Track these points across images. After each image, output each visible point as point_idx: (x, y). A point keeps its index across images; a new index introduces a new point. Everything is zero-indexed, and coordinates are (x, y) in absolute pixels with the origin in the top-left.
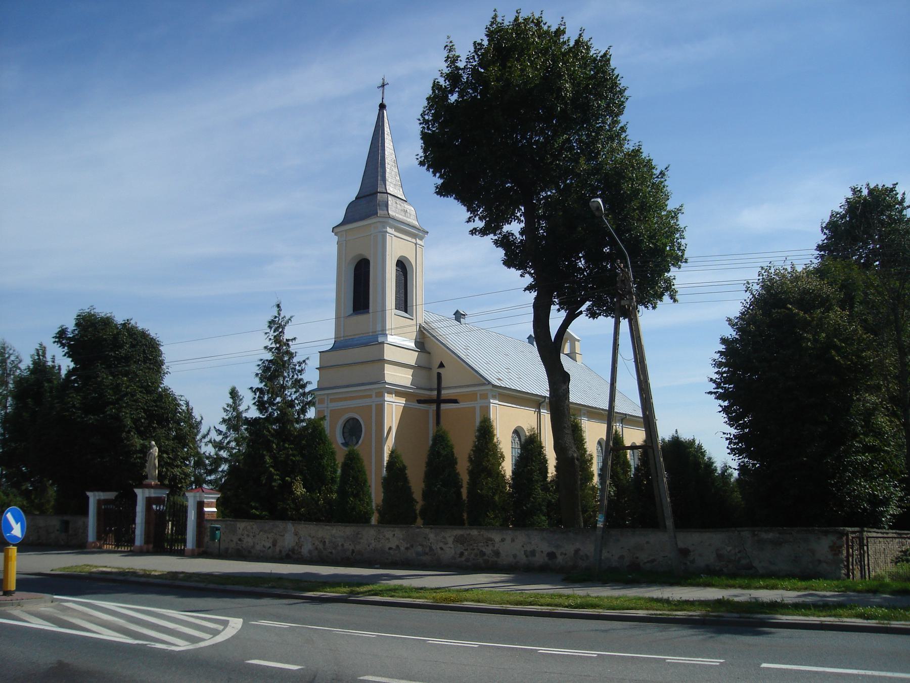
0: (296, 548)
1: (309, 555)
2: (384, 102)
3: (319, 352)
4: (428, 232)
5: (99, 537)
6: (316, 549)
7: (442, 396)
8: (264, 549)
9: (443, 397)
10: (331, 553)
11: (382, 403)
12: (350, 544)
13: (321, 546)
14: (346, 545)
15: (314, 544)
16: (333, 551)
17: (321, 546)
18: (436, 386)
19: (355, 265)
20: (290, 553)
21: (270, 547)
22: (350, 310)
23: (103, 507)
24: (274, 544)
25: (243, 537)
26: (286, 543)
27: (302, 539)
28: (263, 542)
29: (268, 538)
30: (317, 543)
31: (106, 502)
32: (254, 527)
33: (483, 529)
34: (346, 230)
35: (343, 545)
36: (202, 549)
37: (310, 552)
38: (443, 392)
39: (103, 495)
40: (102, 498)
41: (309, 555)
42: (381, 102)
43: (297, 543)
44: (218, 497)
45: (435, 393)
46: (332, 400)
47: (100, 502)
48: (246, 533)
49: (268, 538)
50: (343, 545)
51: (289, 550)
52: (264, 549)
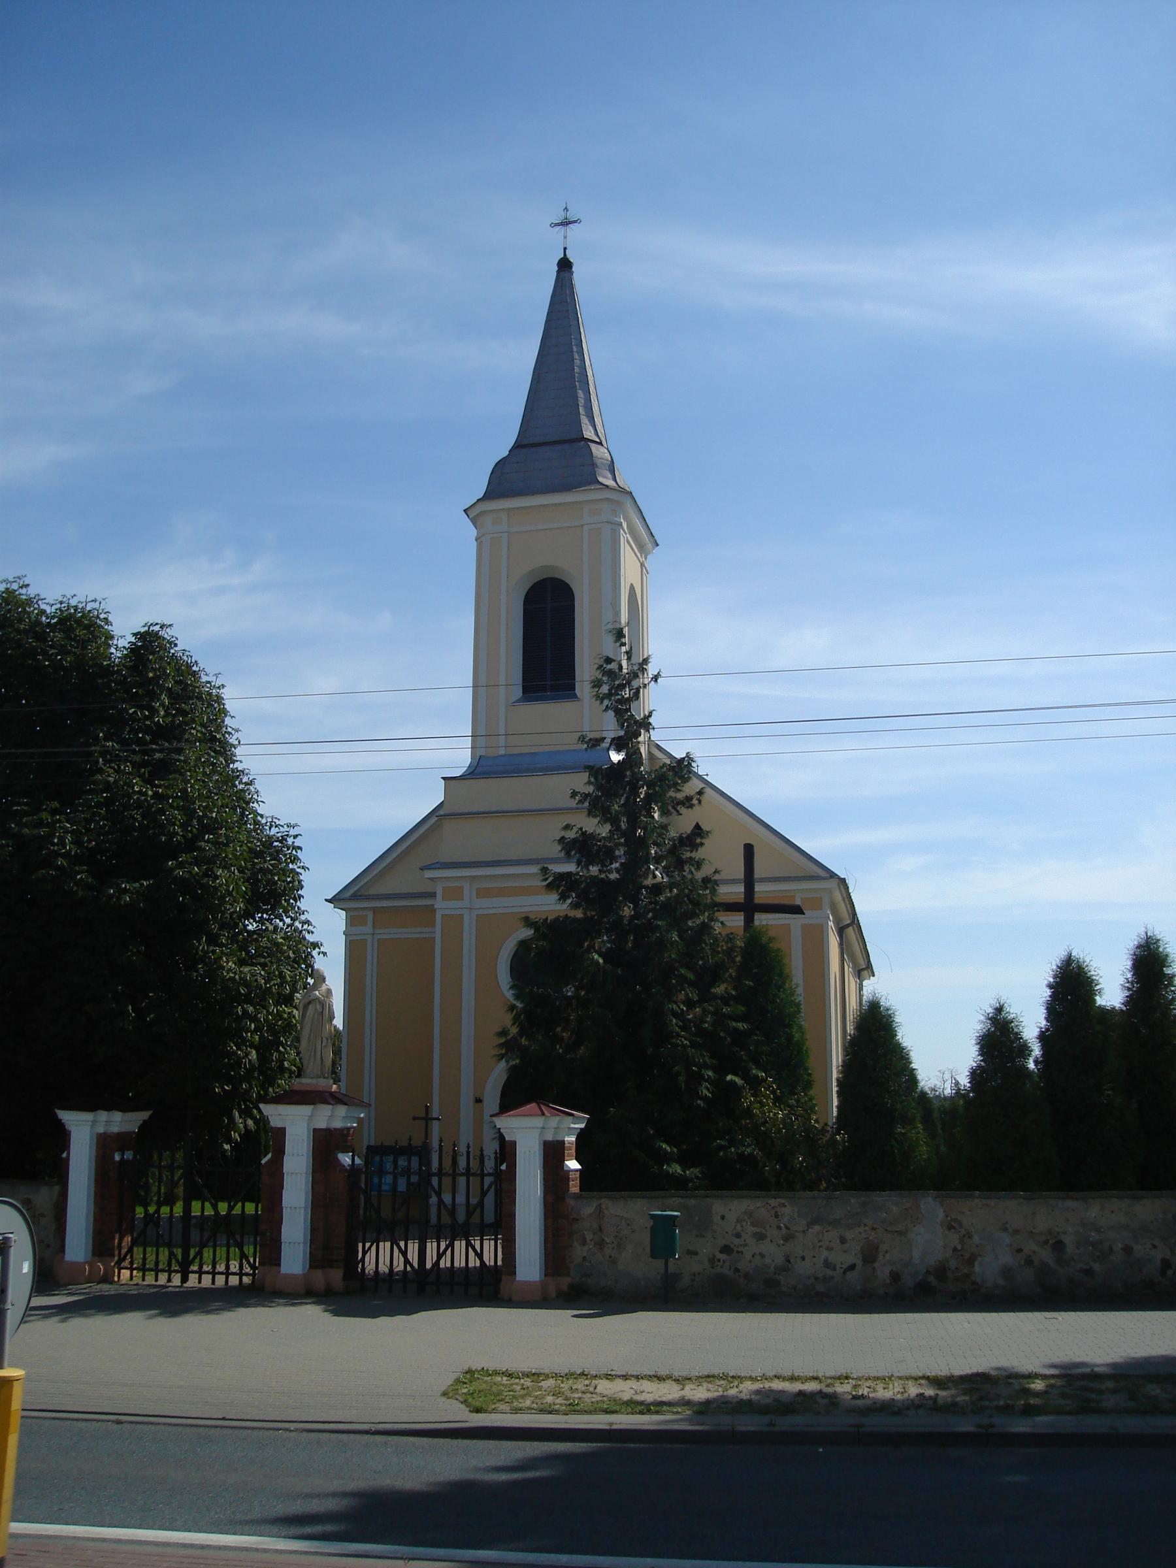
0: (953, 1264)
1: (1001, 1282)
2: (568, 256)
3: (443, 778)
4: (658, 545)
5: (102, 1247)
6: (1029, 1262)
7: (756, 896)
8: (829, 1273)
9: (759, 899)
10: (1089, 1272)
11: (354, 929)
12: (1154, 1246)
13: (1046, 1255)
14: (1139, 1250)
15: (1019, 1251)
16: (1096, 1267)
17: (1046, 1255)
18: (741, 874)
19: (527, 588)
20: (931, 1279)
21: (852, 1267)
22: (518, 692)
23: (117, 1157)
24: (870, 1254)
25: (737, 1241)
26: (916, 1254)
27: (976, 1239)
28: (825, 1253)
29: (843, 1241)
30: (1030, 1246)
31: (120, 1141)
32: (787, 1210)
33: (638, 1197)
34: (509, 510)
35: (1128, 1250)
36: (565, 1282)
37: (1007, 1272)
38: (758, 888)
39: (118, 1122)
40: (115, 1129)
41: (1001, 1282)
42: (562, 256)
43: (955, 1249)
44: (581, 1129)
45: (741, 888)
46: (483, 893)
47: (105, 1144)
48: (751, 1229)
49: (843, 1241)
50: (1128, 1250)
51: (928, 1272)
52: (829, 1273)
